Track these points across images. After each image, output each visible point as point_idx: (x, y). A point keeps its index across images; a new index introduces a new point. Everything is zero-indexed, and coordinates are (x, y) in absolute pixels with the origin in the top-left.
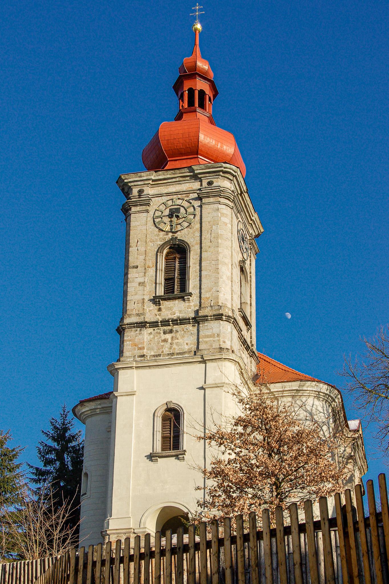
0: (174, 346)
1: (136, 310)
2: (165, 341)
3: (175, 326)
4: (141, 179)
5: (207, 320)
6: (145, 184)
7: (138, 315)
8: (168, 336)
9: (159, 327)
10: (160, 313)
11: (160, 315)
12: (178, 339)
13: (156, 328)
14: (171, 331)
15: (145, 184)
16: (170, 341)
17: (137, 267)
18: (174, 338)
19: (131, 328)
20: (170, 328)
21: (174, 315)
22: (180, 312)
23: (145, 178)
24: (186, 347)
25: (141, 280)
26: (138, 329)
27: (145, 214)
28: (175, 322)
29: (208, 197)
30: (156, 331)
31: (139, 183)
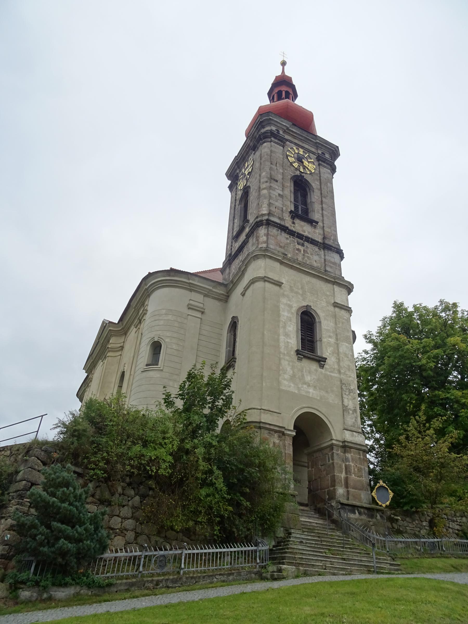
0: (306, 258)
2: (298, 250)
7: (279, 218)
11: (294, 227)
12: (308, 254)
13: (291, 237)
14: (303, 245)
17: (277, 181)
19: (274, 226)
20: (302, 241)
22: (309, 232)
23: (284, 124)
25: (281, 193)
29: (324, 162)
30: (292, 239)
31: (279, 125)
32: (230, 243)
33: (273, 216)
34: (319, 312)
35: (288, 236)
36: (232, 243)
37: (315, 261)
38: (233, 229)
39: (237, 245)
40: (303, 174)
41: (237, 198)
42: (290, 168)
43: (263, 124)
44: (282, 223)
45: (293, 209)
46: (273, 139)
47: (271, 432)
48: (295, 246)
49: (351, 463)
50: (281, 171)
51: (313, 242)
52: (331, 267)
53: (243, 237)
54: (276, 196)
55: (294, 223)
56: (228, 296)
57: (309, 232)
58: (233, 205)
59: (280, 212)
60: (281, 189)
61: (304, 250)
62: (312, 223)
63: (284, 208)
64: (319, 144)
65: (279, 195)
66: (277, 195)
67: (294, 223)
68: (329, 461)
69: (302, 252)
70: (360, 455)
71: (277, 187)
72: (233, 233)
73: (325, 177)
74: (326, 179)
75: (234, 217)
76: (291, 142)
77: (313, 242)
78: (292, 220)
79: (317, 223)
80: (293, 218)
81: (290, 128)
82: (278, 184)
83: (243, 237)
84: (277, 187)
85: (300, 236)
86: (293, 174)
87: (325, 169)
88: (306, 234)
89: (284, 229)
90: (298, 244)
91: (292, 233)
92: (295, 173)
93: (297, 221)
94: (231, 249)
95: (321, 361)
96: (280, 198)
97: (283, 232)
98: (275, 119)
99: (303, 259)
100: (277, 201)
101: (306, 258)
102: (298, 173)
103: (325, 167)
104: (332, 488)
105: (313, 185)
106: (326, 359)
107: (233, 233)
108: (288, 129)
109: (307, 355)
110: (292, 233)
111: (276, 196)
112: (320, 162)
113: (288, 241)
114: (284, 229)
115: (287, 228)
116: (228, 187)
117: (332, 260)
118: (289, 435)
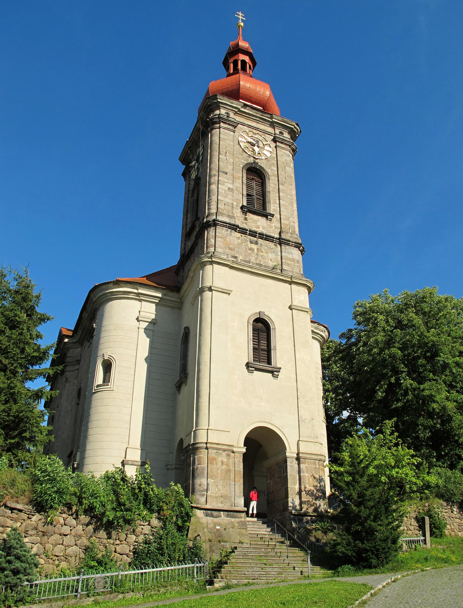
0: (260, 258)
1: (226, 211)
2: (251, 249)
3: (259, 239)
4: (232, 105)
5: (288, 245)
6: (232, 110)
7: (229, 216)
8: (254, 247)
9: (246, 235)
10: (247, 223)
11: (246, 223)
12: (262, 252)
13: (243, 235)
14: (256, 243)
15: (232, 110)
16: (256, 251)
17: (226, 174)
18: (259, 251)
19: (223, 226)
21: (259, 229)
22: (263, 228)
23: (235, 106)
24: (271, 263)
25: (231, 186)
26: (229, 230)
27: (232, 133)
28: (261, 236)
29: (282, 143)
32: (184, 240)
33: (222, 214)
34: (272, 317)
35: (239, 235)
36: (185, 241)
37: (271, 260)
38: (186, 225)
39: (189, 244)
40: (257, 161)
41: (191, 188)
42: (242, 155)
43: (211, 107)
44: (232, 222)
45: (245, 204)
46: (222, 124)
47: (219, 451)
48: (247, 245)
49: (305, 474)
50: (231, 161)
51: (267, 238)
52: (288, 265)
53: (193, 238)
54: (225, 191)
55: (246, 219)
56: (182, 303)
57: (263, 228)
58: (187, 196)
59: (230, 208)
60: (231, 182)
61: (258, 249)
62: (266, 215)
63: (235, 204)
64: (276, 123)
65: (229, 189)
66: (227, 189)
67: (246, 219)
68: (284, 474)
69: (256, 251)
70: (316, 465)
71: (226, 181)
72: (186, 229)
73: (283, 160)
74: (283, 162)
75: (187, 211)
76: (243, 124)
77: (267, 238)
78: (244, 216)
79: (273, 216)
80: (245, 213)
81: (241, 109)
82: (228, 176)
83: (193, 238)
84: (226, 181)
85: (253, 234)
86: (246, 162)
87: (283, 150)
88: (260, 230)
89: (234, 227)
90: (251, 242)
91: (243, 231)
92: (247, 160)
93: (250, 216)
94: (185, 248)
95: (274, 372)
96: (230, 193)
97: (233, 231)
98: (224, 102)
99: (256, 259)
100: (226, 197)
101: (260, 258)
102: (251, 160)
103: (283, 148)
104: (286, 500)
105: (269, 171)
106: (280, 368)
107: (186, 229)
108: (239, 110)
109: (258, 367)
110: (243, 231)
111: (225, 191)
112: (278, 144)
113: (240, 241)
114: (234, 227)
115: (238, 226)
116: (182, 175)
117: (290, 256)
118: (239, 452)
